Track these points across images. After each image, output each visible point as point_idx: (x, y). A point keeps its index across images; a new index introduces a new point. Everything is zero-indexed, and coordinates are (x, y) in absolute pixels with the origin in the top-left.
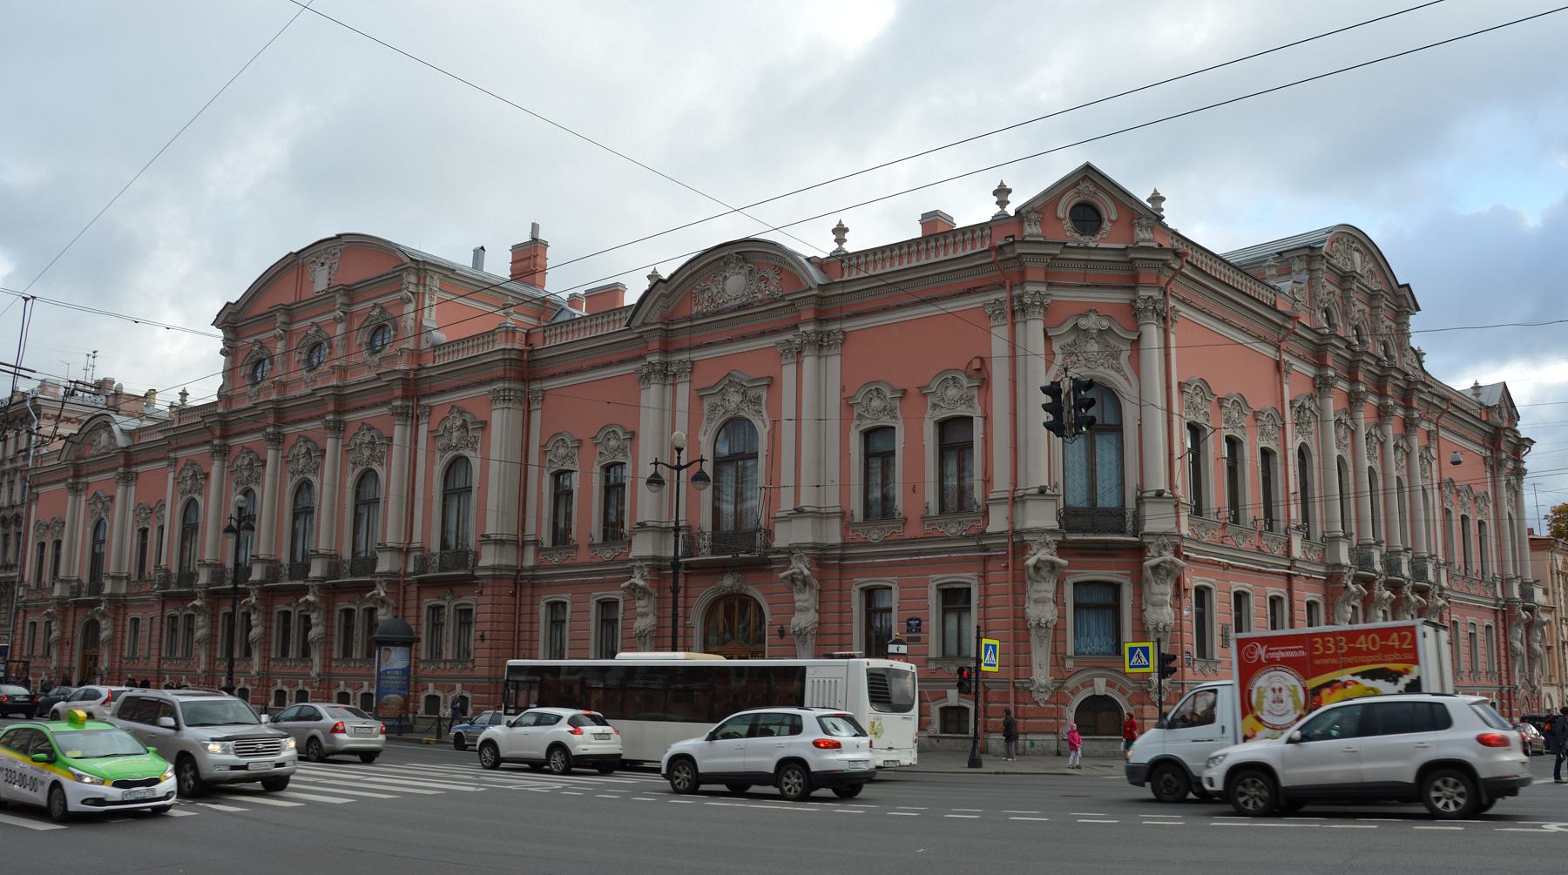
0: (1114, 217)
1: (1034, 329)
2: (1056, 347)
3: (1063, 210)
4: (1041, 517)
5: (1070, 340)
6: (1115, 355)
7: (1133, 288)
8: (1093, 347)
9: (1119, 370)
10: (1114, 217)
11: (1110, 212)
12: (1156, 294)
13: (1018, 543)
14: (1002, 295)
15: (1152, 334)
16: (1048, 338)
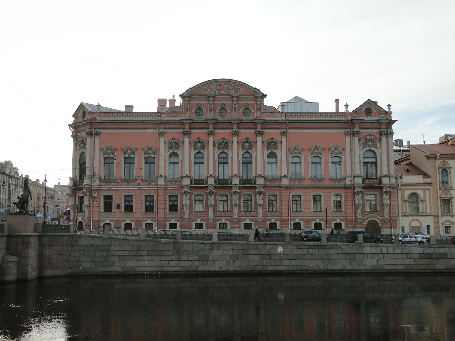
0: (375, 111)
1: (356, 138)
2: (361, 143)
3: (363, 110)
4: (359, 181)
5: (365, 141)
6: (376, 145)
7: (380, 129)
8: (370, 143)
9: (376, 148)
10: (375, 111)
11: (374, 110)
12: (385, 130)
13: (353, 186)
14: (349, 130)
15: (384, 139)
16: (359, 141)
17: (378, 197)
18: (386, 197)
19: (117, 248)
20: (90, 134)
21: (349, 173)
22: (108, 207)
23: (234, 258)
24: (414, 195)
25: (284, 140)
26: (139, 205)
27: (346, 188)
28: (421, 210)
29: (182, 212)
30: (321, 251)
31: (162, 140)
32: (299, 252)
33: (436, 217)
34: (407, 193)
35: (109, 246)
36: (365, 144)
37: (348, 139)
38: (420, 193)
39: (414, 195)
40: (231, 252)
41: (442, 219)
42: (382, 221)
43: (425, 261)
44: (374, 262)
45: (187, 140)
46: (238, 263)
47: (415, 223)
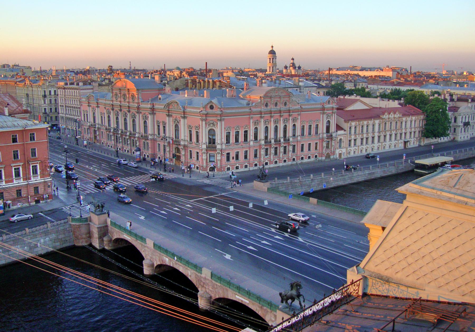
17: (330, 142)
18: (333, 142)
19: (281, 187)
20: (221, 120)
21: (321, 132)
22: (228, 159)
23: (319, 184)
24: (341, 139)
25: (299, 117)
26: (241, 156)
27: (320, 139)
28: (342, 146)
29: (260, 157)
30: (343, 177)
31: (251, 121)
32: (337, 179)
33: (347, 148)
34: (339, 138)
35: (278, 187)
36: (327, 118)
37: (321, 116)
38: (342, 138)
39: (341, 139)
40: (317, 183)
41: (349, 149)
42: (331, 152)
43: (369, 176)
44: (357, 179)
45: (262, 120)
46: (320, 187)
47: (340, 152)
